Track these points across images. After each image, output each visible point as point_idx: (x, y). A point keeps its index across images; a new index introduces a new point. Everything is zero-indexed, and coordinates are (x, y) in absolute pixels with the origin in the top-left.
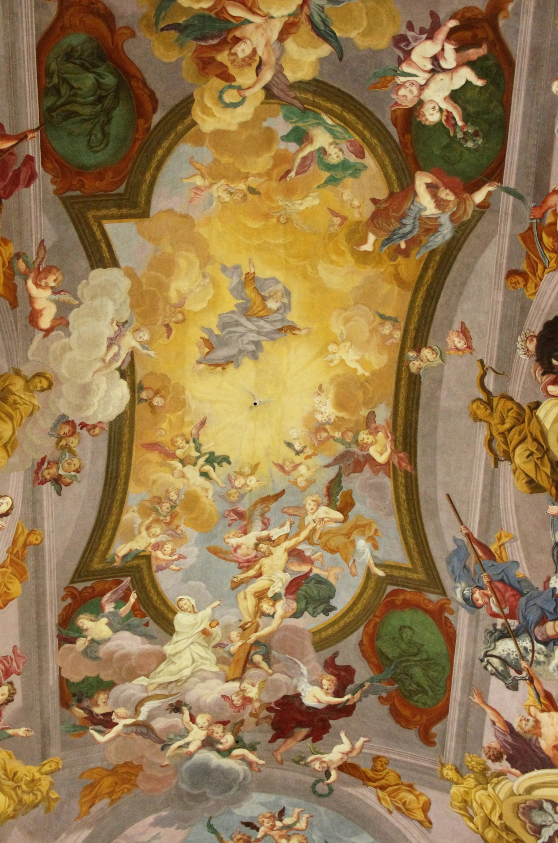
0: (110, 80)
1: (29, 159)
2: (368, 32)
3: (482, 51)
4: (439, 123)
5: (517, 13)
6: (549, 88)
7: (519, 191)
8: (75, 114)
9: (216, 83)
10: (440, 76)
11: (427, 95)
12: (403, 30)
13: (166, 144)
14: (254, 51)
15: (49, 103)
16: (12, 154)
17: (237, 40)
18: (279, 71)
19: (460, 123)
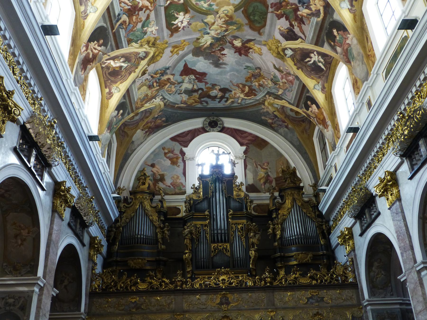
0: (252, 17)
1: (272, 7)
2: (196, 25)
3: (173, 27)
4: (179, 13)
5: (168, 35)
6: (159, 28)
7: (160, 7)
8: (260, 13)
9: (229, 14)
10: (181, 21)
11: (183, 17)
12: (190, 26)
13: (241, 4)
14: (220, 20)
15: (265, 16)
16: (275, 10)
17: (224, 21)
18: (215, 17)
19: (175, 14)
